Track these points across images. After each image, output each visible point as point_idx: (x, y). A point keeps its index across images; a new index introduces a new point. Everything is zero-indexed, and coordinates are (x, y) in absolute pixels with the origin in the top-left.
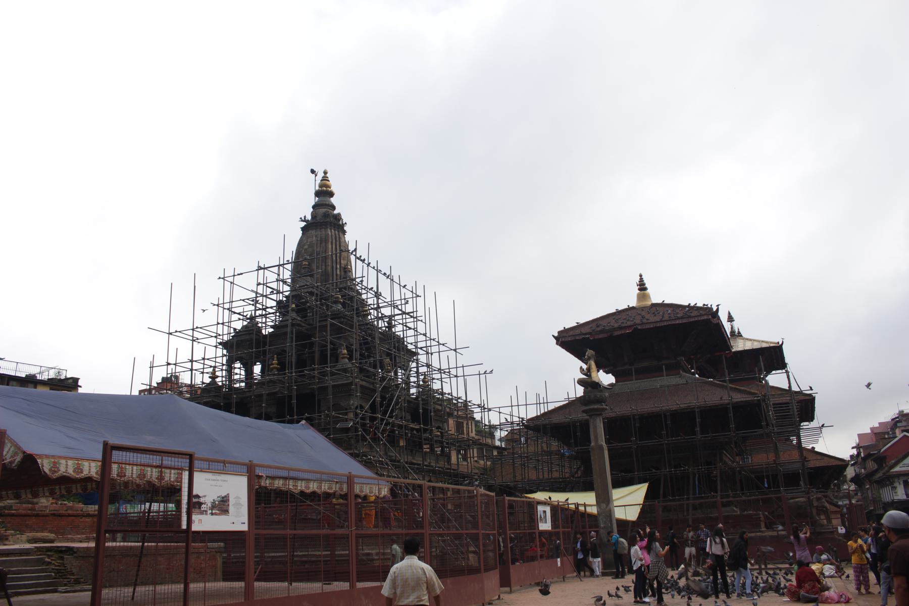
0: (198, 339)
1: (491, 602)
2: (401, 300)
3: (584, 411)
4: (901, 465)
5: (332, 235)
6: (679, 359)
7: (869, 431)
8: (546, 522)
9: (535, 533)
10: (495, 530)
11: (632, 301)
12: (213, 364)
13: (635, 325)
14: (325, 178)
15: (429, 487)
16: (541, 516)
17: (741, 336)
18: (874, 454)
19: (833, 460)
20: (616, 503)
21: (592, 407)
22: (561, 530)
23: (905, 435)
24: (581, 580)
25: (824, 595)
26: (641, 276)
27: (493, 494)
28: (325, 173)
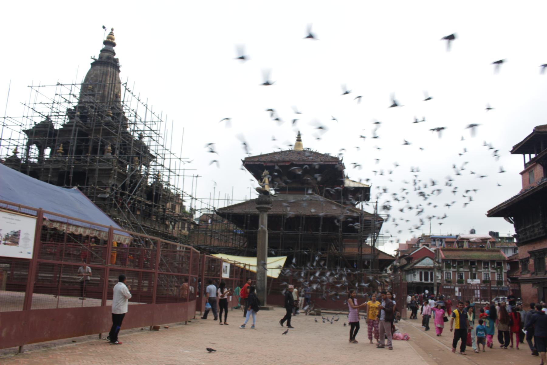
0: (7, 125)
1: (190, 320)
3: (257, 208)
4: (420, 263)
5: (111, 72)
7: (405, 243)
9: (219, 279)
10: (197, 275)
12: (16, 144)
14: (111, 34)
16: (224, 270)
18: (406, 256)
19: (388, 256)
20: (268, 266)
22: (234, 279)
23: (424, 248)
25: (395, 335)
27: (199, 252)
28: (112, 30)
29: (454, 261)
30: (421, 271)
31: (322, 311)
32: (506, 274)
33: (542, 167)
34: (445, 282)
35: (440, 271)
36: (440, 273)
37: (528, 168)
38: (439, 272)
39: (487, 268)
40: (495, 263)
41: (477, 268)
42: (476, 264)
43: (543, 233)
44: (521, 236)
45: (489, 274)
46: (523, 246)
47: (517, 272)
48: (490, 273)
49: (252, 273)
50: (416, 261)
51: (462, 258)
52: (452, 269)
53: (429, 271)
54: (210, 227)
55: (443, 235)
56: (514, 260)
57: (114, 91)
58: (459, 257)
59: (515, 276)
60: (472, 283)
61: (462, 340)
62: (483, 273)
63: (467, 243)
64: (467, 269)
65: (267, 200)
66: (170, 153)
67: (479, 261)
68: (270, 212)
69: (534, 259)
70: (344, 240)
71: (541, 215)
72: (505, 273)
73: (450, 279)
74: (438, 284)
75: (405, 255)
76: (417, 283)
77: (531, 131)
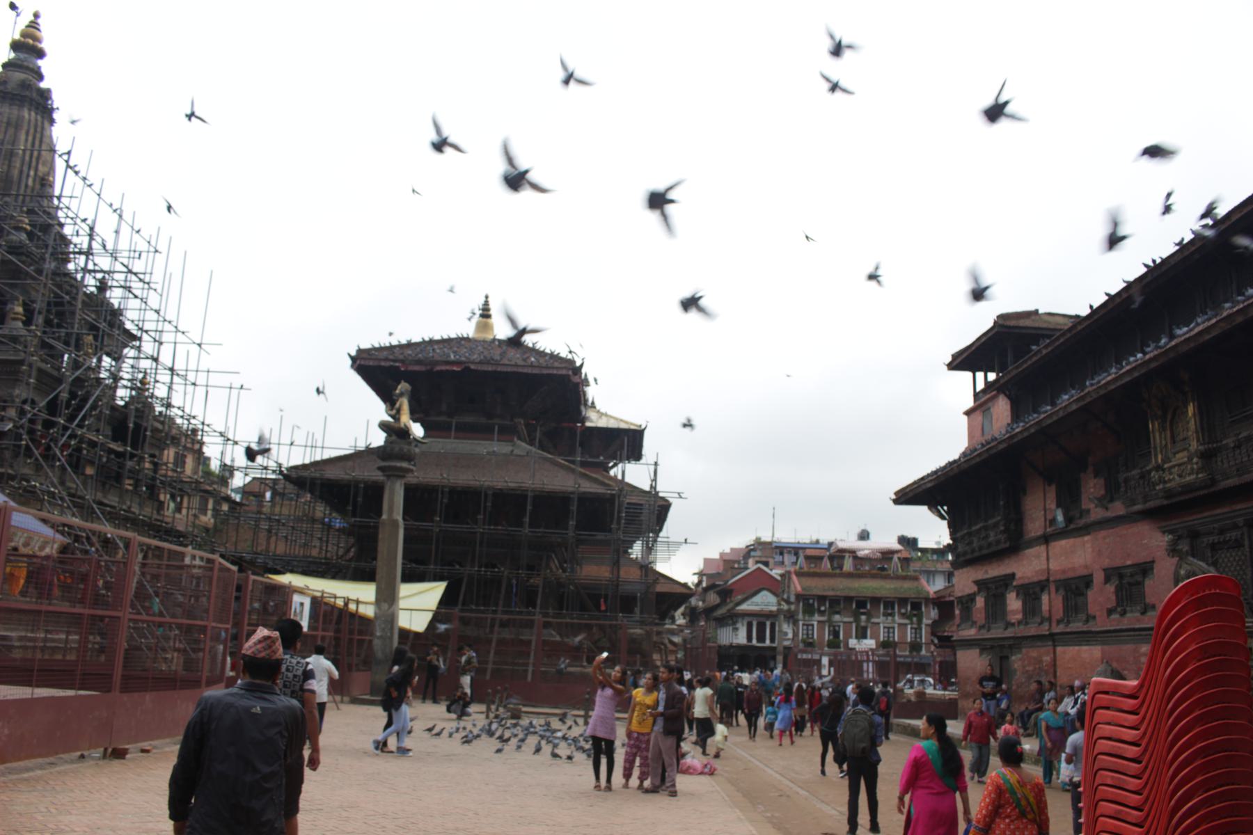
2: (130, 251)
3: (380, 469)
4: (749, 602)
6: (516, 420)
7: (717, 556)
10: (228, 624)
11: (468, 329)
13: (468, 363)
15: (141, 545)
16: (295, 609)
17: (595, 407)
18: (719, 585)
19: (677, 586)
21: (399, 464)
23: (759, 569)
24: (338, 709)
25: (685, 763)
26: (487, 297)
27: (235, 568)
29: (822, 599)
30: (749, 619)
31: (525, 709)
32: (929, 629)
33: (1009, 402)
34: (801, 646)
35: (791, 621)
36: (791, 625)
37: (982, 404)
40: (907, 605)
41: (869, 615)
42: (869, 606)
43: (1005, 542)
44: (960, 549)
45: (894, 628)
46: (965, 570)
47: (951, 623)
48: (896, 626)
49: (364, 620)
50: (740, 597)
51: (838, 593)
52: (817, 617)
54: (266, 510)
55: (801, 541)
56: (947, 599)
57: (36, 170)
58: (833, 590)
60: (858, 647)
61: (310, 742)
62: (882, 626)
63: (851, 559)
64: (848, 617)
65: (405, 450)
66: (174, 329)
67: (876, 601)
68: (409, 479)
69: (985, 597)
70: (581, 547)
71: (1002, 503)
72: (927, 625)
73: (813, 638)
74: (787, 648)
75: (717, 583)
76: (739, 647)
77: (990, 324)
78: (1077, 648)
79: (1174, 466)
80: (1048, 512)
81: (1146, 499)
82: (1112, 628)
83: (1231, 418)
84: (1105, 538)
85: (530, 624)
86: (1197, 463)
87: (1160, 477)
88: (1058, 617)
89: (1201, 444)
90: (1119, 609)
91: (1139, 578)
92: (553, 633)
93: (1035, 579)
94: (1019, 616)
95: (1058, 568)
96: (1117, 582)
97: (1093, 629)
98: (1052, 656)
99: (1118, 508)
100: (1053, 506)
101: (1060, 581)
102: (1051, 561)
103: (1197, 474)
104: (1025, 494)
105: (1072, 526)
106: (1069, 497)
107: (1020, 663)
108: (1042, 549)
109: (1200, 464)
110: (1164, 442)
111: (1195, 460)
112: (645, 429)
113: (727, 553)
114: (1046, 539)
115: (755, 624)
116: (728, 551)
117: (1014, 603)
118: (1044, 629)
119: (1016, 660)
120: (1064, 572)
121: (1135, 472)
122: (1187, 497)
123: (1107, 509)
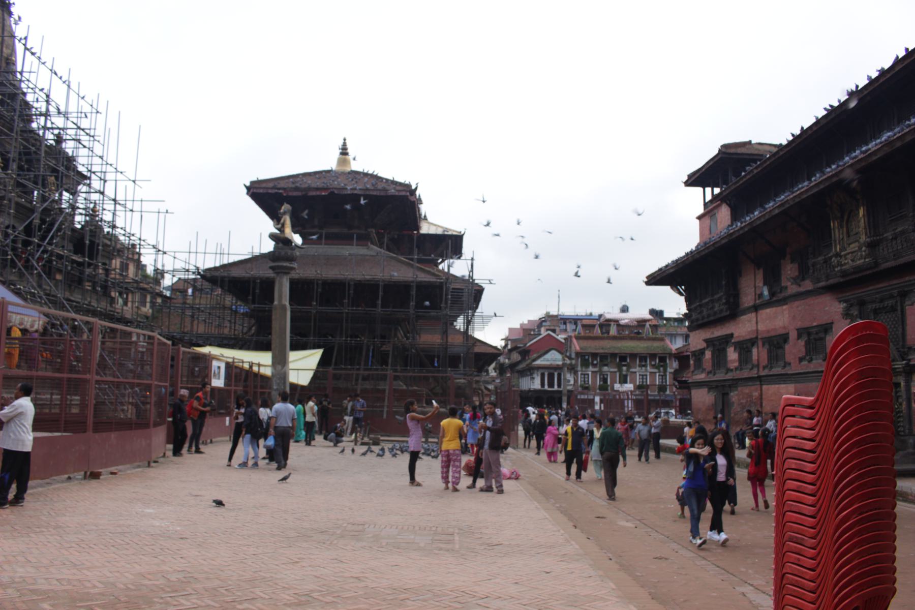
2: (78, 112)
3: (271, 268)
4: (542, 359)
6: (369, 230)
7: (518, 327)
8: (219, 378)
10: (167, 382)
13: (332, 188)
16: (214, 373)
17: (426, 219)
18: (520, 347)
19: (490, 348)
20: (291, 366)
22: (233, 388)
23: (549, 335)
26: (345, 140)
27: (169, 342)
29: (595, 355)
30: (542, 371)
31: (382, 438)
32: (672, 376)
33: (729, 209)
34: (580, 389)
35: (573, 372)
36: (572, 375)
38: (571, 373)
39: (644, 366)
42: (628, 360)
43: (726, 311)
44: (694, 316)
45: (646, 375)
46: (697, 332)
48: (648, 374)
49: (264, 378)
50: (535, 355)
51: (606, 351)
52: (591, 369)
53: (556, 371)
54: (190, 301)
56: (685, 354)
58: (602, 349)
59: (686, 377)
60: (621, 389)
62: (638, 374)
65: (289, 254)
66: (115, 170)
67: (633, 356)
68: (294, 275)
71: (724, 283)
72: (670, 373)
73: (588, 383)
75: (519, 346)
76: (536, 391)
77: (716, 152)
78: (777, 386)
79: (848, 254)
80: (757, 289)
81: (828, 278)
82: (802, 371)
83: (890, 217)
84: (798, 306)
85: (384, 378)
86: (865, 251)
87: (838, 261)
88: (764, 364)
89: (868, 237)
90: (807, 358)
91: (822, 335)
92: (401, 383)
93: (748, 337)
94: (736, 364)
95: (764, 329)
96: (806, 339)
97: (789, 372)
98: (759, 392)
99: (808, 285)
100: (761, 284)
101: (765, 338)
102: (759, 324)
103: (865, 259)
104: (741, 276)
105: (775, 299)
106: (773, 278)
107: (736, 397)
108: (753, 315)
109: (867, 252)
110: (841, 237)
111: (864, 249)
112: (463, 235)
113: (526, 324)
114: (756, 308)
115: (546, 374)
116: (526, 322)
117: (732, 355)
118: (754, 373)
119: (734, 396)
120: (768, 331)
121: (820, 259)
122: (857, 276)
123: (800, 285)
